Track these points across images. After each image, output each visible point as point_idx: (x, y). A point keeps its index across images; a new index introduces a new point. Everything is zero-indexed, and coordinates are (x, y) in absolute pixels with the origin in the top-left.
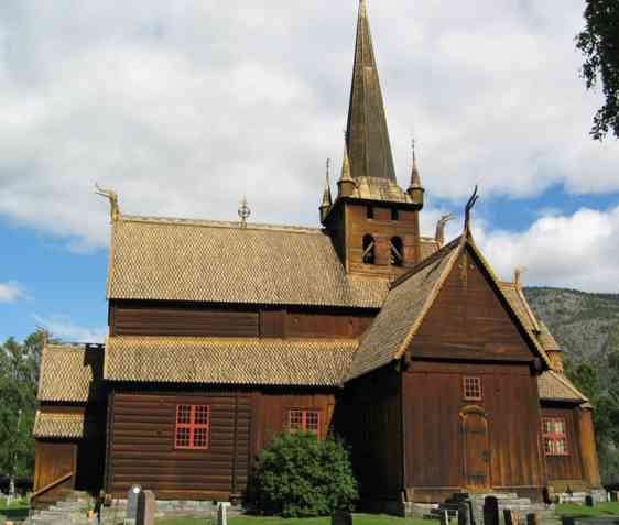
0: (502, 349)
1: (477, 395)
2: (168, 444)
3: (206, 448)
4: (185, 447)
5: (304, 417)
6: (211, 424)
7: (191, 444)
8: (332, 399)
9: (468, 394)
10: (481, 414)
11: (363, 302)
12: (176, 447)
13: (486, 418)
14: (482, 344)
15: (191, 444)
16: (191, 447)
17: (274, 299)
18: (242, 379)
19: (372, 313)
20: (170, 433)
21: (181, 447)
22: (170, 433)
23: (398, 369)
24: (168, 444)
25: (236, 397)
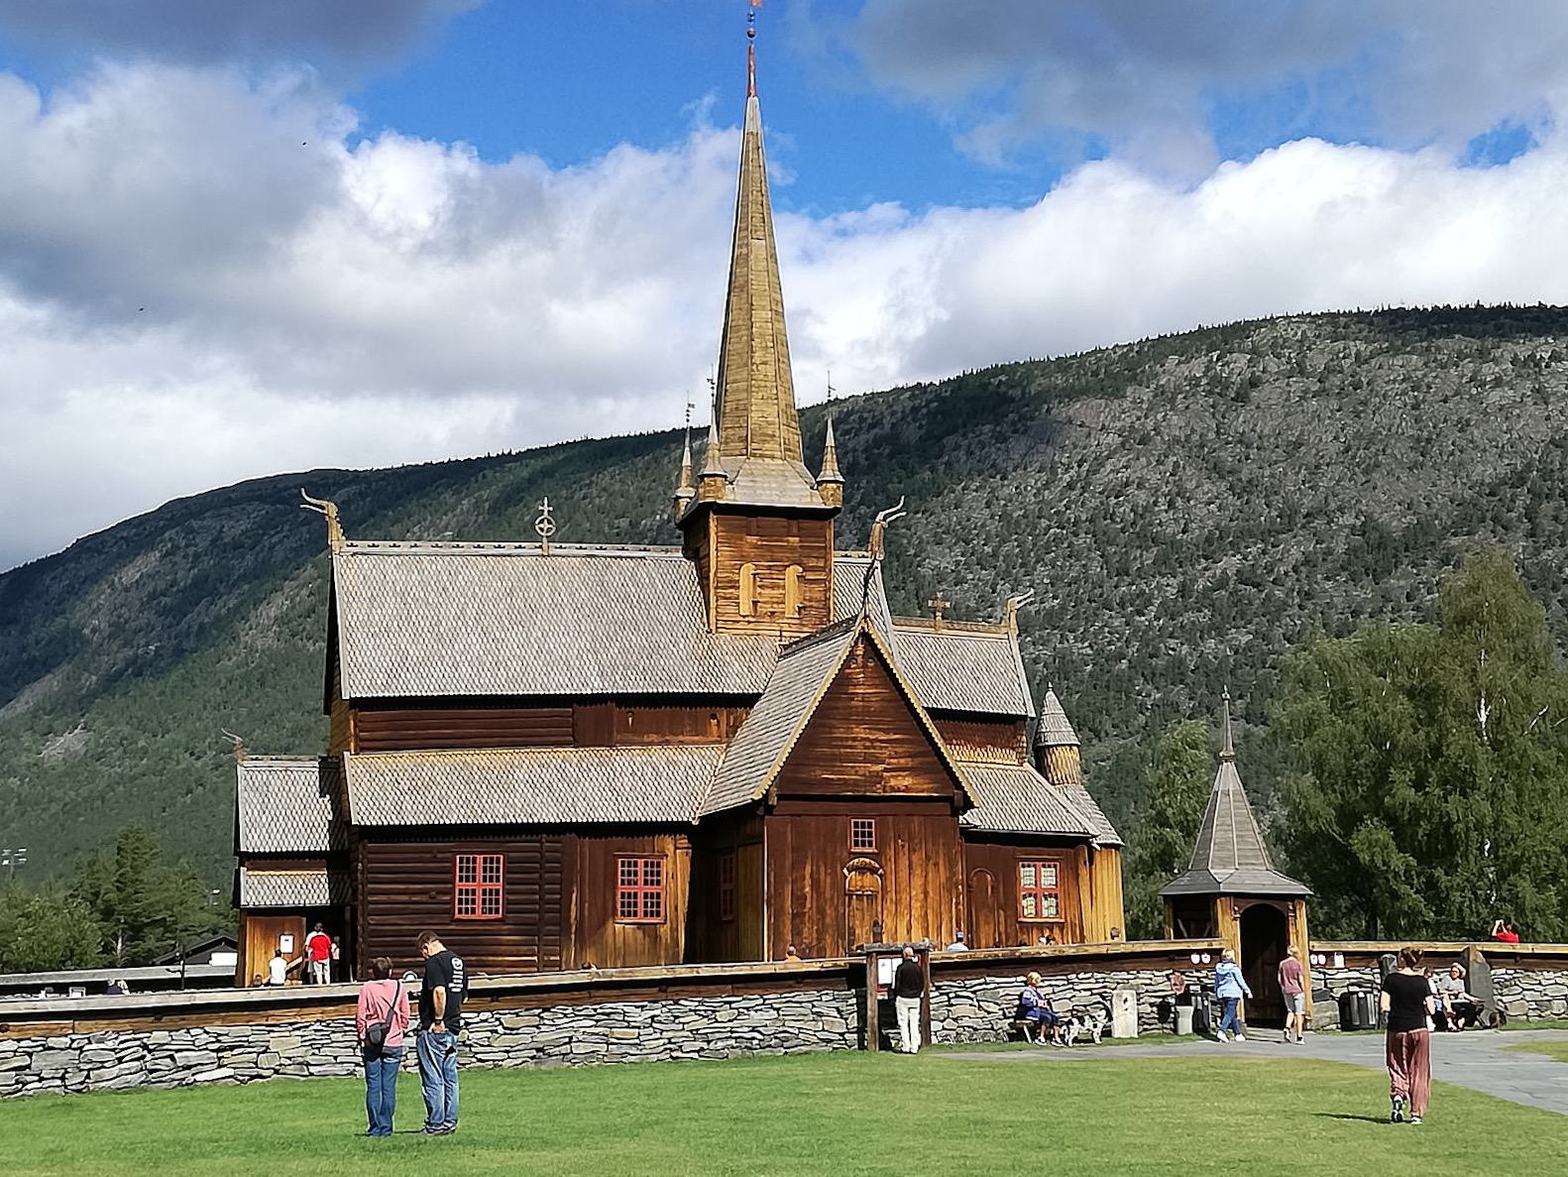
0: (903, 782)
1: (870, 845)
2: (446, 912)
3: (500, 916)
4: (470, 916)
5: (641, 869)
6: (507, 882)
7: (479, 911)
8: (684, 842)
9: (856, 844)
10: (874, 871)
11: (733, 686)
12: (457, 916)
13: (880, 876)
14: (878, 778)
15: (479, 911)
16: (479, 915)
17: (595, 686)
18: (549, 815)
19: (748, 701)
20: (448, 898)
21: (463, 916)
22: (448, 898)
23: (760, 812)
24: (446, 912)
25: (540, 841)
